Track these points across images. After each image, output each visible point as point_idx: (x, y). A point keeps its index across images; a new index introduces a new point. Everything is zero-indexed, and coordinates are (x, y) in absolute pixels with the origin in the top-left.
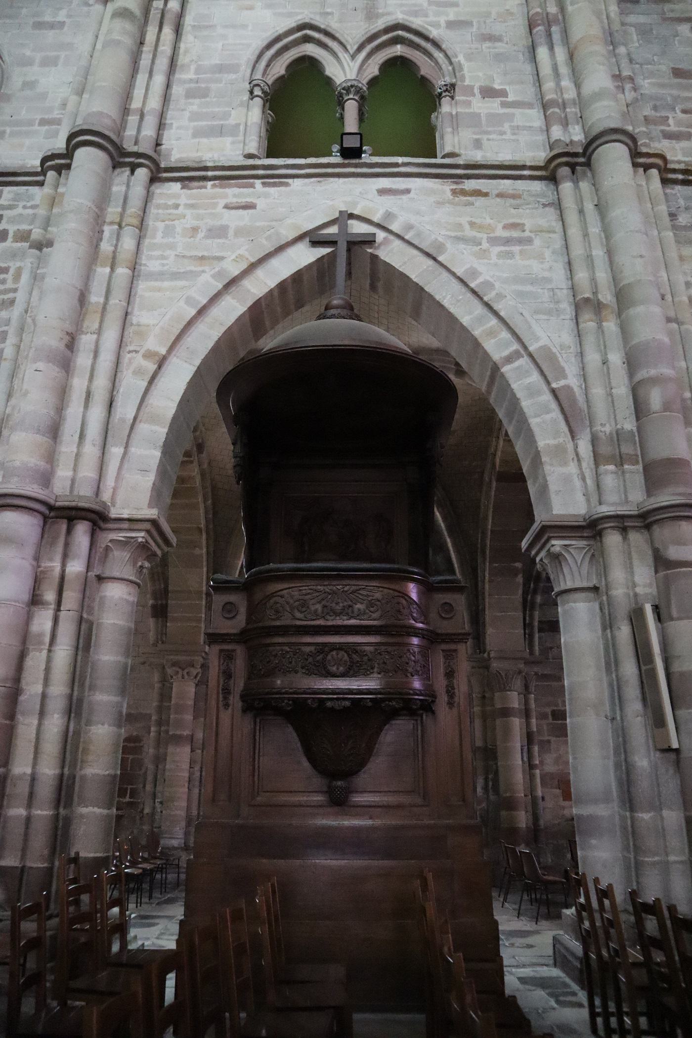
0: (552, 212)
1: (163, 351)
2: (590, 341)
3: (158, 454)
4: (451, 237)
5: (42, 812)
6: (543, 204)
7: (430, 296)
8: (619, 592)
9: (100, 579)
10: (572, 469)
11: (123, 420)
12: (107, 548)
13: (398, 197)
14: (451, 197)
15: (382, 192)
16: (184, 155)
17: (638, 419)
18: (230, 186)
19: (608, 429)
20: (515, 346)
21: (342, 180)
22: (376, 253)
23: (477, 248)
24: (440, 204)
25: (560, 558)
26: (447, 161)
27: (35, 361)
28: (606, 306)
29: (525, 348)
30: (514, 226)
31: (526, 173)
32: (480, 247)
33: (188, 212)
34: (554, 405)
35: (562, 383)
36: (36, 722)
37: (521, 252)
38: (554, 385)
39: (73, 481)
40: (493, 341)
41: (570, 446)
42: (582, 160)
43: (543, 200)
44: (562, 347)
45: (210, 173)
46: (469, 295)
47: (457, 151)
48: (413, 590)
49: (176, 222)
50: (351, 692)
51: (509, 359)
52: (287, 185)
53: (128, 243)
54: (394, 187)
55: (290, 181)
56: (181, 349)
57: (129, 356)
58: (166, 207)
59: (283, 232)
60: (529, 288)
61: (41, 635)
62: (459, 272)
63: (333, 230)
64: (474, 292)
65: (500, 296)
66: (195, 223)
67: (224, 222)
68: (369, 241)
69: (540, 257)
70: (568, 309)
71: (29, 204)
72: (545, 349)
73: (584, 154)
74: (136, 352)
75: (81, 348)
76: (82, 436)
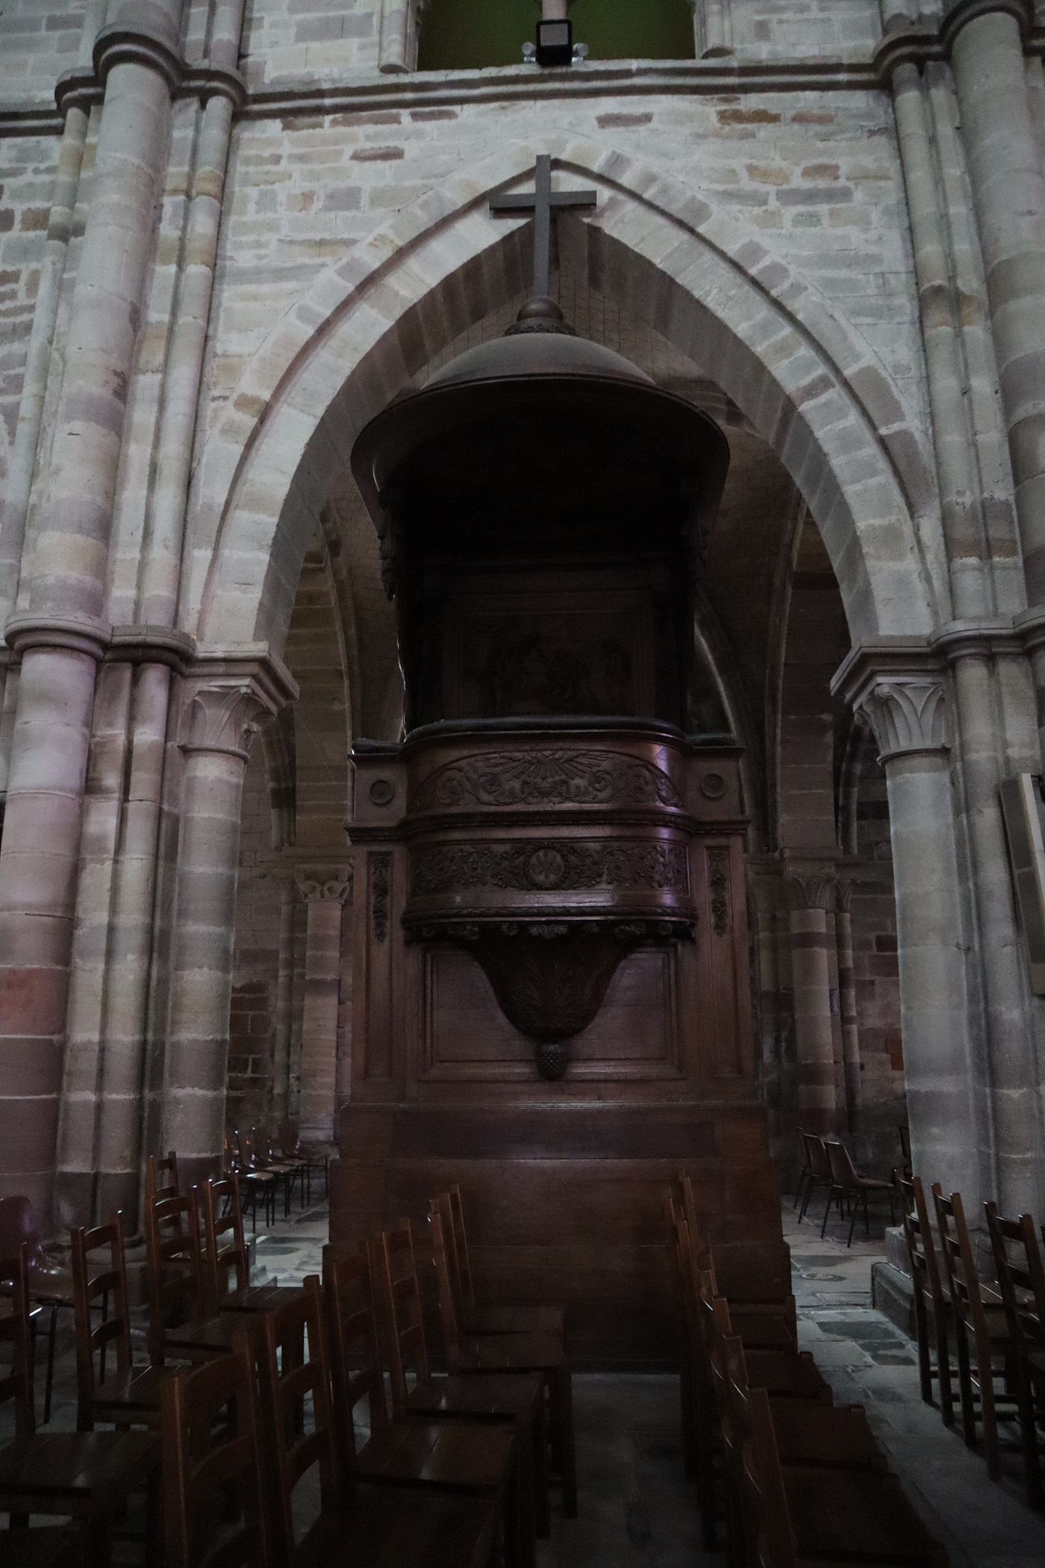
1: (266, 395)
2: (941, 357)
3: (265, 557)
4: (718, 192)
5: (120, 1096)
7: (687, 294)
8: (981, 756)
9: (187, 751)
10: (910, 564)
11: (209, 507)
12: (195, 705)
14: (719, 125)
15: (606, 121)
16: (285, 72)
17: (1017, 482)
18: (359, 122)
19: (967, 499)
20: (821, 370)
21: (540, 103)
23: (758, 211)
24: (701, 137)
25: (890, 703)
26: (712, 62)
27: (69, 418)
28: (969, 299)
29: (837, 371)
31: (842, 77)
32: (764, 208)
33: (296, 168)
34: (882, 463)
35: (896, 427)
36: (101, 966)
38: (883, 431)
39: (137, 604)
40: (785, 362)
41: (907, 528)
43: (871, 124)
44: (897, 367)
45: (328, 102)
46: (748, 289)
48: (660, 757)
49: (277, 187)
50: (567, 911)
51: (811, 391)
52: (451, 115)
53: (202, 224)
54: (625, 111)
55: (456, 108)
56: (294, 394)
57: (213, 405)
58: (259, 161)
59: (448, 194)
60: (843, 273)
61: (101, 839)
62: (732, 249)
63: (528, 188)
64: (755, 283)
66: (307, 186)
67: (352, 183)
68: (586, 204)
69: (864, 223)
70: (905, 304)
71: (42, 166)
72: (869, 372)
74: (225, 398)
75: (139, 395)
76: (147, 534)
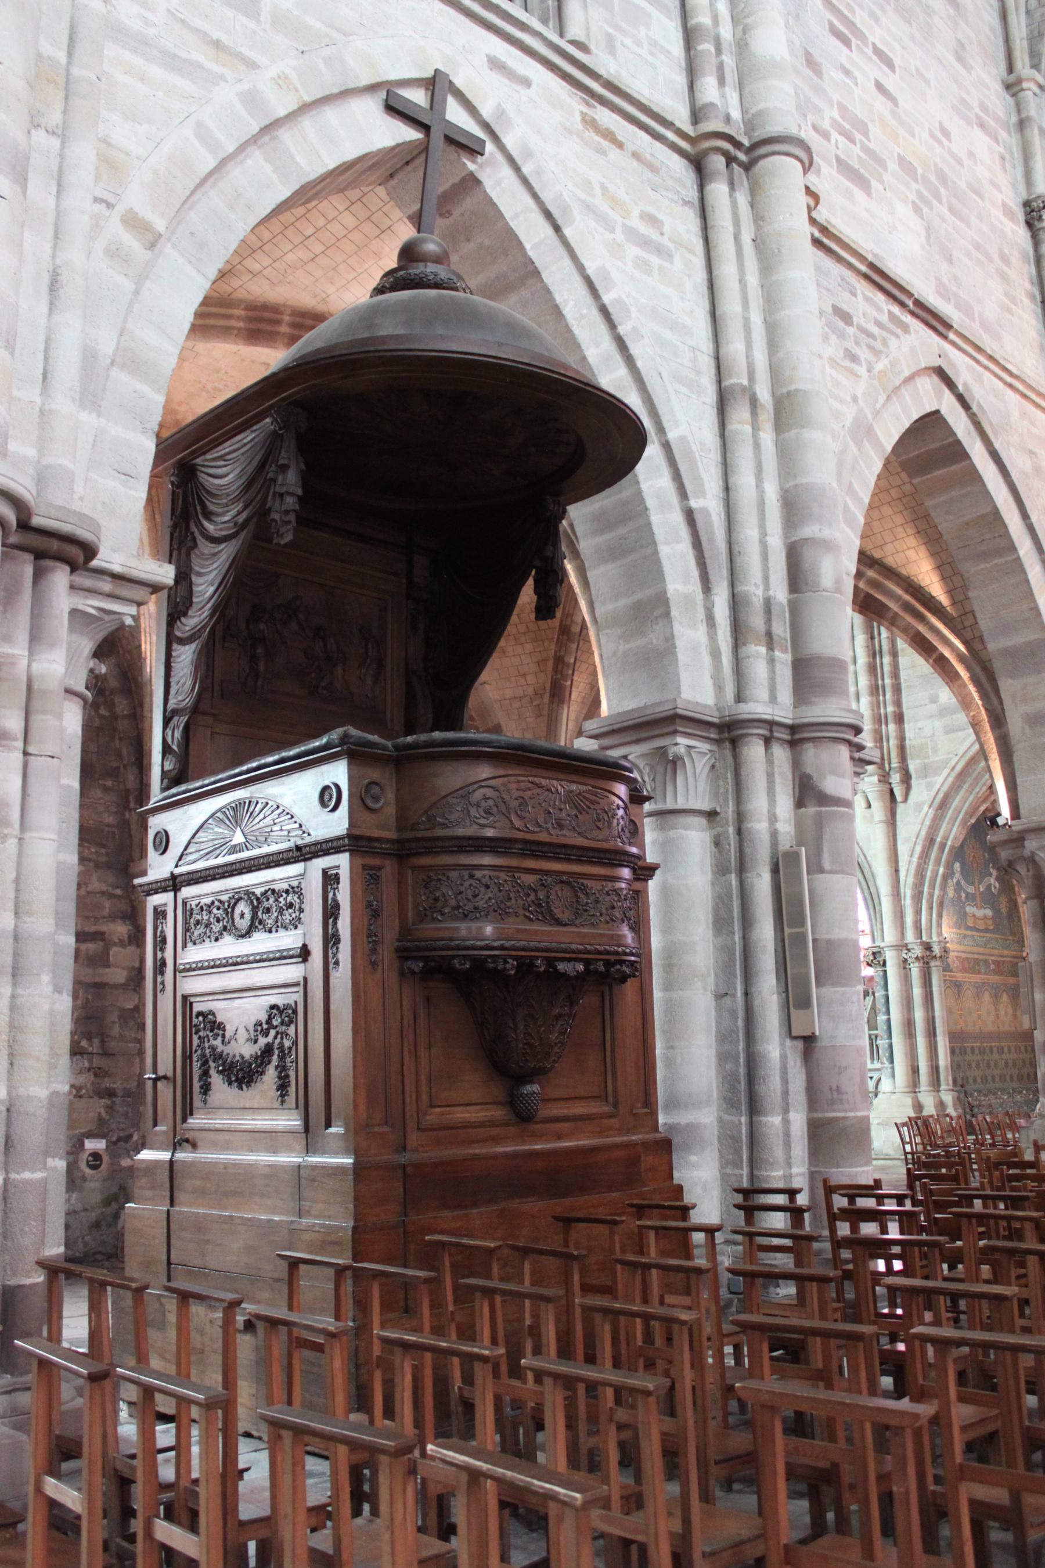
4: (579, 199)
6: (683, 199)
13: (514, 86)
14: (581, 127)
15: (496, 64)
25: (679, 763)
26: (571, 50)
30: (650, 219)
31: (670, 135)
37: (661, 269)
42: (742, 156)
60: (668, 334)
63: (418, 97)
64: (604, 311)
68: (472, 149)
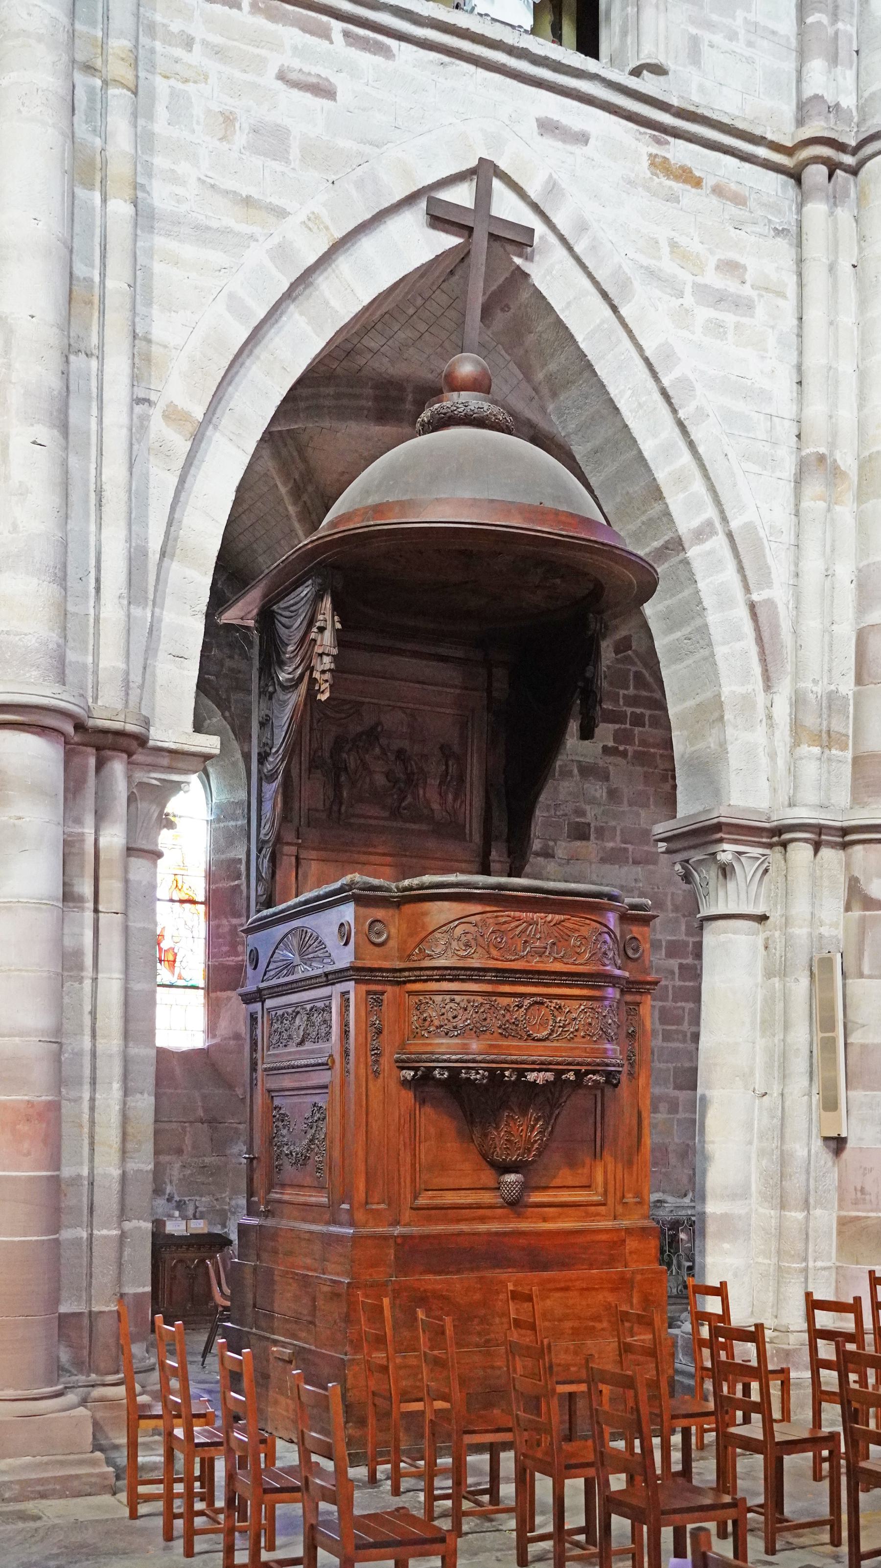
0: (784, 247)
1: (198, 413)
6: (775, 229)
10: (759, 736)
13: (569, 147)
14: (649, 175)
15: (547, 127)
20: (710, 512)
21: (482, 73)
22: (526, 266)
23: (676, 302)
29: (724, 519)
30: (731, 267)
31: (762, 152)
32: (681, 301)
33: (212, 66)
37: (737, 326)
38: (755, 597)
40: (681, 496)
41: (761, 699)
46: (657, 396)
47: (660, 59)
49: (190, 88)
52: (386, 52)
58: (170, 39)
65: (701, 414)
72: (750, 528)
73: (855, 151)
